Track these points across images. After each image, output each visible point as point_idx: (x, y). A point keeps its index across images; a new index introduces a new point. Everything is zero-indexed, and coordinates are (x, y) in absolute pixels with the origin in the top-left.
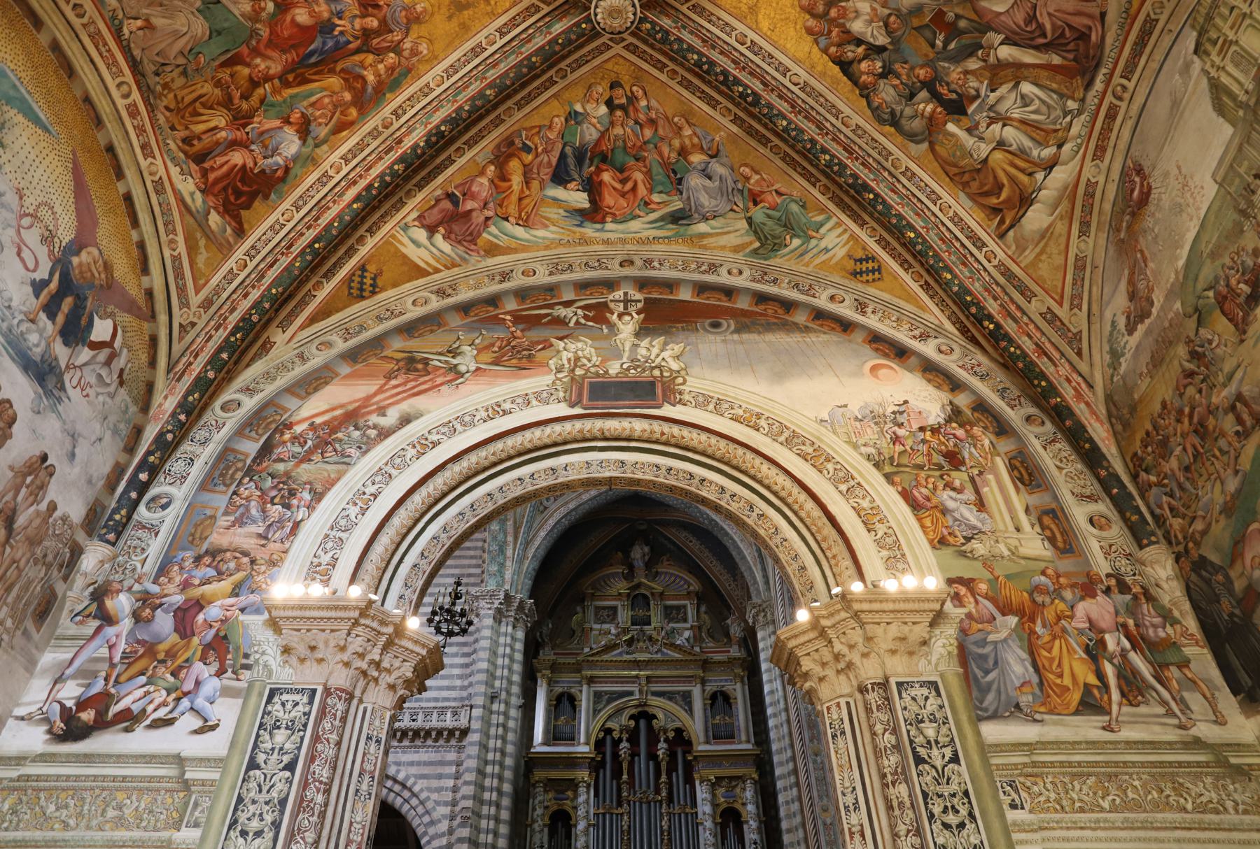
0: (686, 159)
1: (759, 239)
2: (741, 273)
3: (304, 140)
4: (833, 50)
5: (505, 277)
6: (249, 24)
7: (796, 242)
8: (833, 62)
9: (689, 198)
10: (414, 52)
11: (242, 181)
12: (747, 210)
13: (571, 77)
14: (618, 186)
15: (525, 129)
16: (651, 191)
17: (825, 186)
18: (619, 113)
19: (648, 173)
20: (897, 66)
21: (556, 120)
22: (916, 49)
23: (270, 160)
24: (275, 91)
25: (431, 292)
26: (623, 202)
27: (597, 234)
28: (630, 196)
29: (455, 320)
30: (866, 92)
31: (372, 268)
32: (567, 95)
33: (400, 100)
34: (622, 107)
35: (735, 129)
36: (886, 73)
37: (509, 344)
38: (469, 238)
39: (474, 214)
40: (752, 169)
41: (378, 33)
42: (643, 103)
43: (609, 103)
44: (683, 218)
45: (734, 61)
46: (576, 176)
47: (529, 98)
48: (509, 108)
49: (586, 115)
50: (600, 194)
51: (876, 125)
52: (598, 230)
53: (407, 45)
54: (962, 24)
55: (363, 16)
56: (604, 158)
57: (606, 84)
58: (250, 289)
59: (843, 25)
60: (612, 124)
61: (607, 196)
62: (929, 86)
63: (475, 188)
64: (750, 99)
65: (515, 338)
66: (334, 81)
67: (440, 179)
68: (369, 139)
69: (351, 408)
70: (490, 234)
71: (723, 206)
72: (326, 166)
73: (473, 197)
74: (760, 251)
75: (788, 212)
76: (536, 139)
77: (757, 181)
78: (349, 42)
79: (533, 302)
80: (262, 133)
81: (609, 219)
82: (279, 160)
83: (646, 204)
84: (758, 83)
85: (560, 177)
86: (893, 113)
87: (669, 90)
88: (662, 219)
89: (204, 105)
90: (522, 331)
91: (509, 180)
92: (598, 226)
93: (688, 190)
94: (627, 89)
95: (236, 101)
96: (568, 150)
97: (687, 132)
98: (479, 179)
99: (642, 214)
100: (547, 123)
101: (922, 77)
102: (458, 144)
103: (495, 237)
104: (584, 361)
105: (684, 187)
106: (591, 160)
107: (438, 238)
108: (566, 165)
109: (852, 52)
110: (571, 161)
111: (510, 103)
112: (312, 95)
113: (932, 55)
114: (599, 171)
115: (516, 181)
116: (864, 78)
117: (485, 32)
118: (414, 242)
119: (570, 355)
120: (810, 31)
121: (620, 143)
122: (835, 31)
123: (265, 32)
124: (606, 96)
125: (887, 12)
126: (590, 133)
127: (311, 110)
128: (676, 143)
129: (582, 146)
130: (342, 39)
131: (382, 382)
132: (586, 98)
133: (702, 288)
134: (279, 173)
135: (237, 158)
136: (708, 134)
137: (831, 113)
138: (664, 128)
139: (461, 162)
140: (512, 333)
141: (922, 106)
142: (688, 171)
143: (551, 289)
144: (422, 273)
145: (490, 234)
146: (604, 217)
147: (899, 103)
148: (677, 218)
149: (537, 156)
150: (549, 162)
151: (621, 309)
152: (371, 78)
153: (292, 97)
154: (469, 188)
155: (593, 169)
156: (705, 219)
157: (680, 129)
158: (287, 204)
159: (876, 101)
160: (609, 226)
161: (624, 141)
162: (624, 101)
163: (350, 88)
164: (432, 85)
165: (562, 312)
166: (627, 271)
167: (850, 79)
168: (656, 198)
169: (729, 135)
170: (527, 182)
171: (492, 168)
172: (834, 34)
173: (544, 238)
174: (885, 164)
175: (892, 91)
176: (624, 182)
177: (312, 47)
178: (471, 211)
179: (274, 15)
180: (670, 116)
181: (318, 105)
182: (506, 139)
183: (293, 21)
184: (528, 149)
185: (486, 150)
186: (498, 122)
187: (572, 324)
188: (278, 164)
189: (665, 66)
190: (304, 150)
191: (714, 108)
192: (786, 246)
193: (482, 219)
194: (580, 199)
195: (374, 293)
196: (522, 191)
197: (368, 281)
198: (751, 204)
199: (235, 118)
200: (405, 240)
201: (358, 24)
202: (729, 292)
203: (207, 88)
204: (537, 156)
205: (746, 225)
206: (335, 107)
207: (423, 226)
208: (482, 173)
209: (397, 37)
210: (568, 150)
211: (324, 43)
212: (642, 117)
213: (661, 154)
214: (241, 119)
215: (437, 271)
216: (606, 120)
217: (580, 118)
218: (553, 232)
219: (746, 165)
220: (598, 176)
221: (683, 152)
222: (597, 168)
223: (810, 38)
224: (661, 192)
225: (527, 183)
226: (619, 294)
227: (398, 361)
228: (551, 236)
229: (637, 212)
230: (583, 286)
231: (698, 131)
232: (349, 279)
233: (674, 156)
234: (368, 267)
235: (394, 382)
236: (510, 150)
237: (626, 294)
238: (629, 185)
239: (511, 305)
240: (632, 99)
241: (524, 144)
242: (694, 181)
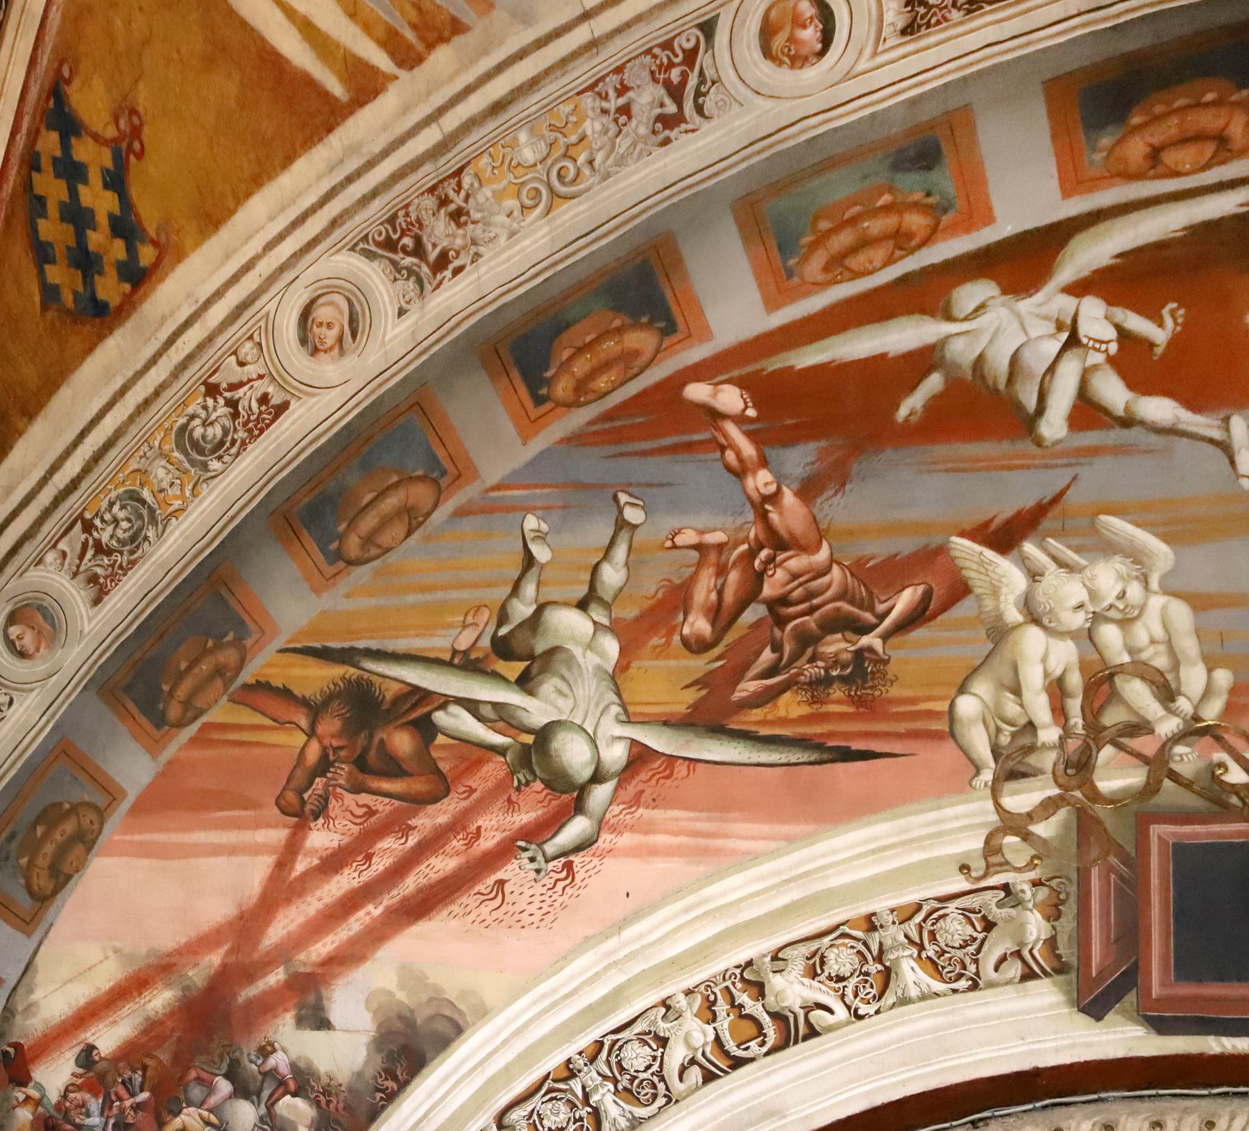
37: (750, 594)
65: (779, 543)
69: (201, 970)
79: (838, 267)
90: (809, 490)
104: (1138, 694)
119: (1064, 655)
131: (278, 835)
140: (762, 505)
187: (1054, 426)
227: (316, 710)
235: (321, 839)
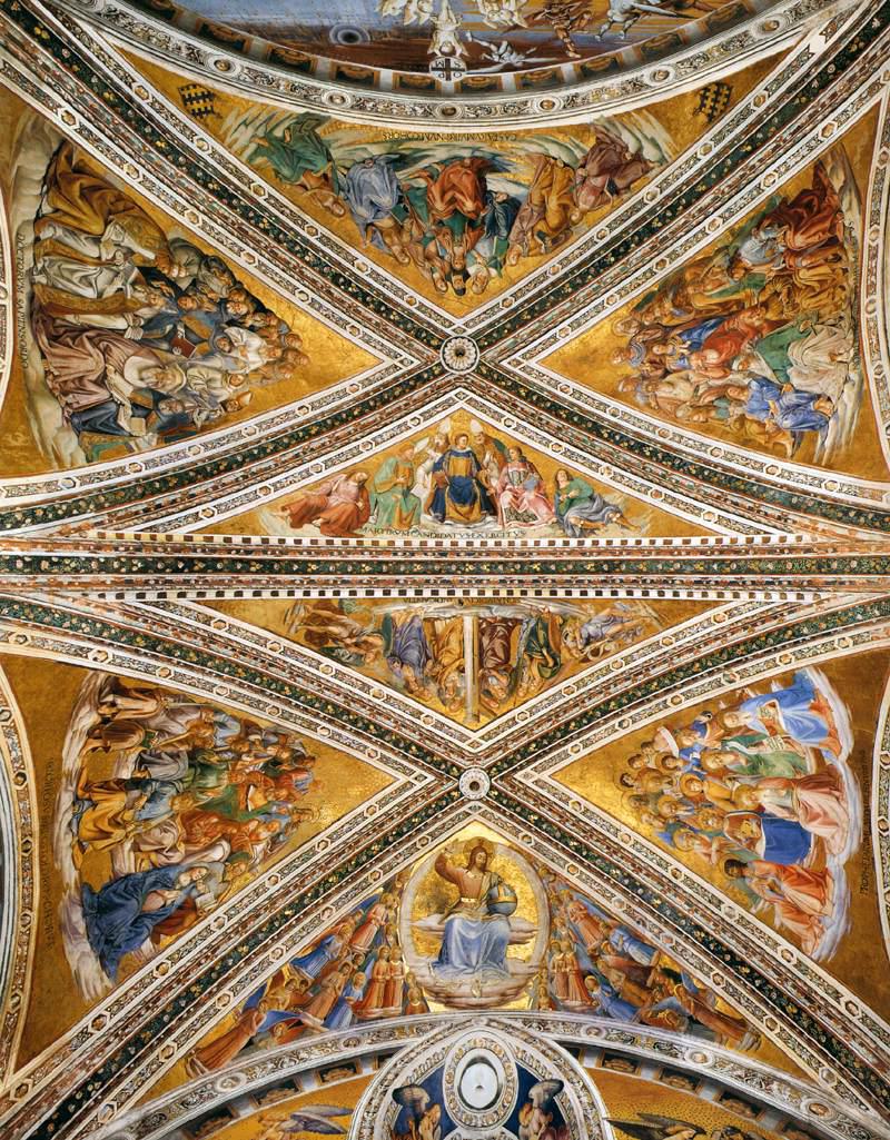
1: (317, 137)
2: (331, 98)
3: (737, 250)
4: (274, 323)
5: (571, 102)
6: (756, 353)
7: (278, 133)
9: (391, 183)
10: (627, 324)
11: (802, 218)
12: (333, 170)
13: (499, 299)
14: (459, 196)
16: (427, 190)
18: (458, 267)
19: (430, 208)
20: (214, 309)
22: (202, 326)
23: (771, 236)
24: (750, 297)
25: (648, 86)
27: (479, 145)
28: (447, 185)
29: (626, 52)
30: (237, 287)
31: (702, 118)
33: (648, 284)
34: (455, 272)
36: (223, 303)
38: (603, 146)
39: (595, 172)
41: (656, 341)
42: (436, 275)
43: (466, 276)
45: (360, 313)
49: (487, 266)
51: (221, 256)
52: (478, 149)
53: (633, 331)
54: (165, 346)
55: (663, 355)
56: (472, 223)
57: (469, 293)
58: (827, 103)
59: (268, 342)
60: (464, 257)
62: (181, 294)
63: (592, 198)
64: (342, 280)
66: (699, 303)
68: (680, 252)
70: (582, 150)
71: (357, 173)
72: (722, 230)
74: (314, 123)
75: (293, 169)
77: (326, 200)
78: (680, 335)
80: (772, 261)
81: (467, 162)
82: (763, 236)
84: (336, 294)
85: (512, 206)
86: (209, 268)
88: (416, 160)
89: (813, 289)
91: (560, 205)
92: (477, 154)
94: (451, 289)
95: (785, 291)
96: (504, 233)
97: (396, 249)
101: (189, 300)
102: (601, 243)
103: (578, 146)
106: (483, 222)
107: (632, 149)
108: (507, 219)
109: (258, 321)
110: (502, 222)
111: (552, 279)
112: (721, 293)
113: (185, 319)
114: (476, 212)
115: (553, 204)
116: (242, 299)
117: (568, 339)
118: (657, 146)
120: (297, 337)
121: (457, 238)
122: (275, 337)
123: (746, 348)
124: (469, 281)
125: (233, 354)
126: (484, 248)
127: (725, 280)
128: (406, 238)
129: (491, 237)
130: (685, 337)
133: (370, 82)
134: (766, 223)
135: (799, 241)
141: (183, 274)
143: (525, 85)
144: (653, 110)
145: (582, 150)
146: (472, 163)
147: (204, 277)
148: (399, 161)
151: (452, 60)
152: (668, 305)
153: (737, 292)
155: (482, 214)
156: (373, 160)
158: (769, 192)
159: (226, 277)
160: (466, 154)
163: (686, 297)
164: (618, 296)
165: (515, 59)
166: (447, 103)
168: (422, 183)
170: (543, 203)
171: (574, 218)
172: (275, 336)
174: (206, 218)
175: (215, 288)
177: (710, 332)
178: (598, 176)
179: (734, 359)
180: (412, 263)
181: (717, 283)
183: (720, 354)
188: (765, 232)
189: (418, 308)
190: (738, 244)
191: (373, 271)
192: (288, 128)
193: (588, 167)
194: (495, 183)
195: (706, 89)
196: (549, 193)
197: (709, 103)
198: (330, 175)
199: (790, 276)
200: (664, 147)
201: (669, 350)
202: (340, 77)
203: (806, 303)
205: (332, 152)
206: (702, 281)
207: (645, 162)
209: (640, 338)
210: (504, 233)
211: (700, 335)
213: (419, 226)
214: (786, 275)
215: (638, 111)
218: (522, 149)
219: (340, 216)
220: (477, 207)
221: (399, 229)
223: (295, 331)
226: (456, 78)
228: (526, 146)
230: (494, 88)
231: (386, 249)
232: (728, 106)
233: (407, 223)
234: (706, 120)
237: (448, 78)
238: (448, 197)
239: (567, 68)
240: (446, 279)
241: (543, 239)
242: (387, 200)
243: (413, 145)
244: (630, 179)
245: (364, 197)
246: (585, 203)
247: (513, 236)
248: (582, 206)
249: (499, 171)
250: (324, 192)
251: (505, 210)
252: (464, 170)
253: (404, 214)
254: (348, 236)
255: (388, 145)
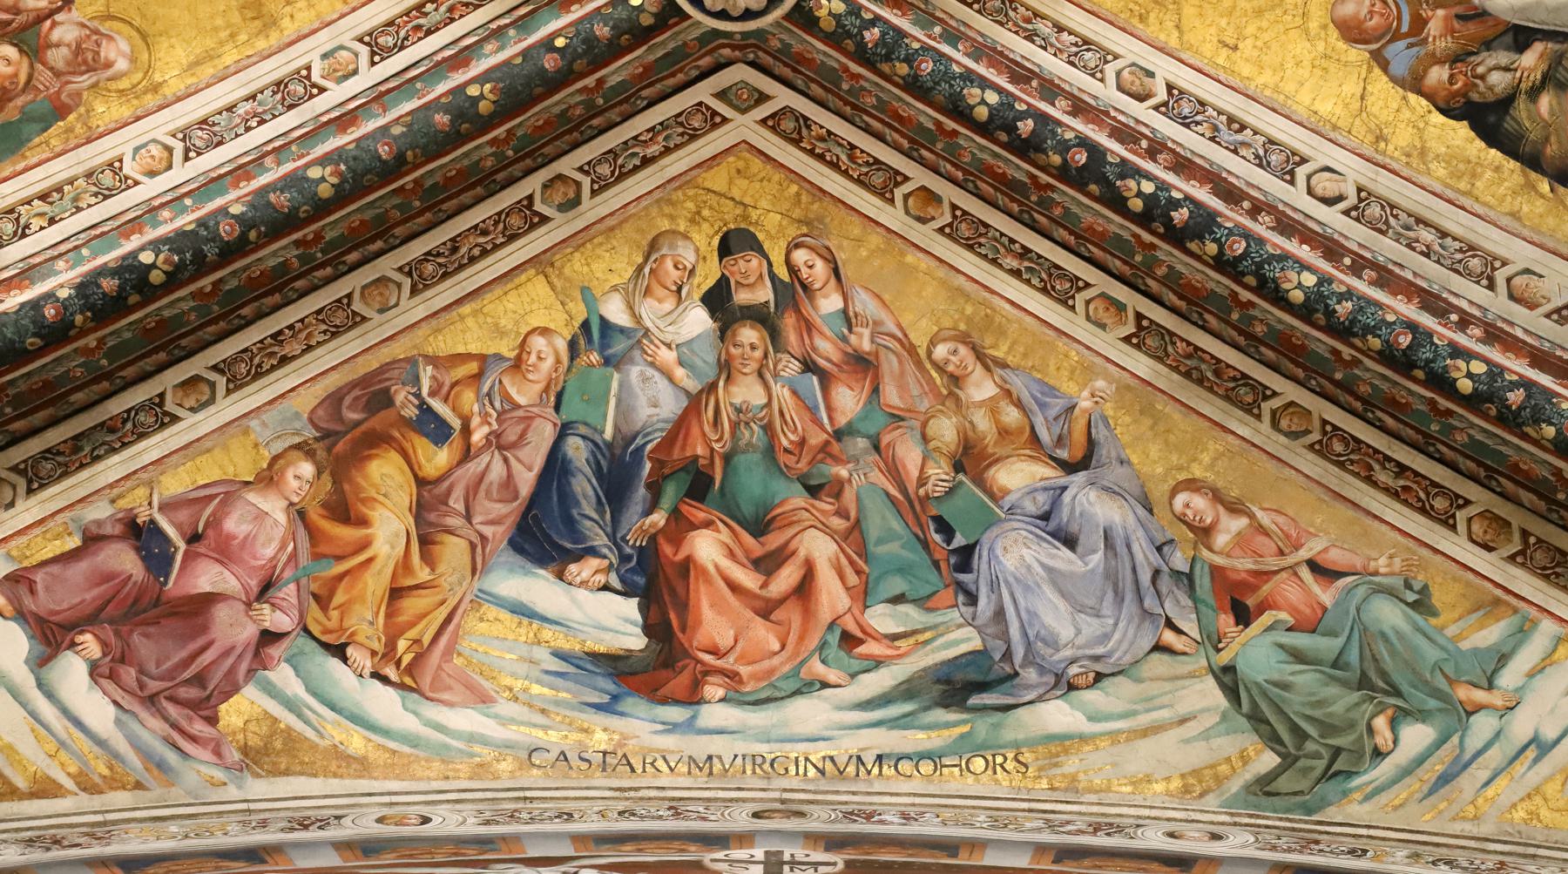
0: (980, 481)
1: (1273, 740)
8: (1445, 112)
9: (1000, 614)
13: (593, 209)
15: (433, 360)
16: (863, 596)
17: (1488, 516)
18: (749, 334)
19: (854, 537)
21: (538, 342)
26: (764, 635)
27: (669, 742)
32: (576, 266)
34: (757, 315)
35: (1142, 365)
39: (222, 614)
40: (1217, 497)
42: (830, 303)
43: (717, 300)
44: (983, 687)
46: (600, 540)
47: (451, 260)
48: (382, 281)
49: (639, 336)
50: (683, 606)
52: (672, 728)
56: (699, 486)
57: (706, 239)
60: (726, 368)
61: (707, 613)
63: (235, 524)
67: (112, 468)
73: (226, 553)
76: (468, 398)
77: (1240, 540)
81: (713, 690)
83: (849, 641)
87: (911, 258)
88: (906, 691)
91: (363, 522)
92: (676, 713)
93: (994, 586)
94: (777, 257)
97: (981, 388)
98: (252, 496)
99: (832, 676)
100: (507, 349)
103: (291, 705)
105: (979, 578)
108: (567, 499)
114: (680, 526)
121: (753, 435)
128: (946, 430)
132: (644, 280)
136: (1052, 391)
137: (1467, 274)
138: (902, 388)
139: (194, 425)
142: (991, 522)
149: (467, 455)
150: (509, 482)
154: (215, 522)
157: (956, 380)
160: (715, 714)
161: (768, 428)
162: (765, 294)
164: (128, 169)
167: (1511, 151)
168: (882, 619)
169: (1123, 389)
170: (427, 539)
171: (307, 469)
173: (472, 738)
176: (767, 564)
178: (209, 600)
180: (920, 340)
182: (364, 381)
184: (438, 431)
185: (285, 403)
186: (340, 320)
191: (1065, 301)
193: (249, 632)
196: (405, 565)
204: (467, 455)
205: (1219, 700)
208: (268, 478)
212: (826, 349)
213: (894, 471)
216: (707, 357)
217: (619, 346)
218: (504, 721)
219: (1192, 485)
220: (677, 542)
222: (675, 514)
224: (898, 599)
225: (426, 542)
229: (818, 668)
231: (1018, 384)
233: (939, 472)
236: (376, 422)
238: (786, 578)
240: (793, 291)
241: (425, 409)
243: (916, 740)
244: (81, 568)
245: (1097, 558)
246: (261, 515)
247: (543, 434)
248: (274, 507)
249: (595, 656)
250: (1248, 564)
251: (571, 525)
252: (728, 663)
253: (946, 511)
254: (1157, 418)
255: (1009, 735)
